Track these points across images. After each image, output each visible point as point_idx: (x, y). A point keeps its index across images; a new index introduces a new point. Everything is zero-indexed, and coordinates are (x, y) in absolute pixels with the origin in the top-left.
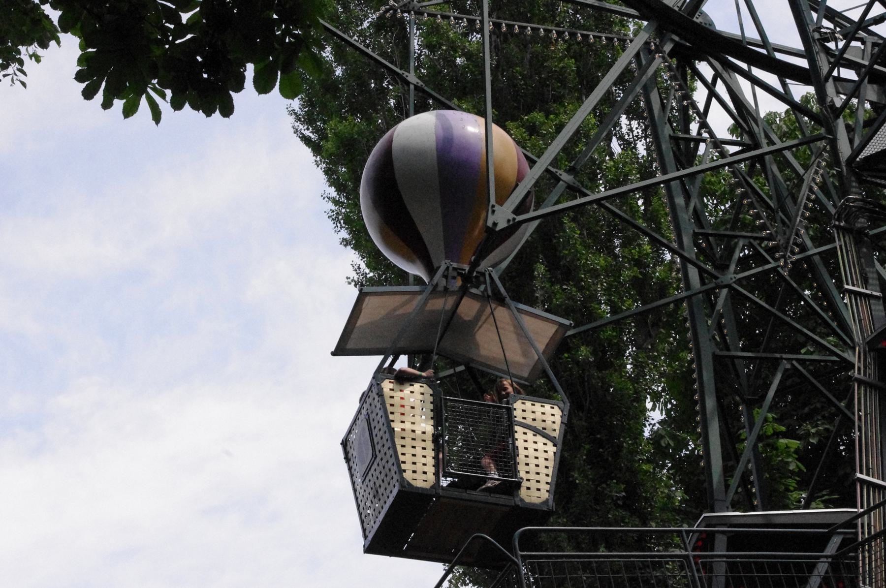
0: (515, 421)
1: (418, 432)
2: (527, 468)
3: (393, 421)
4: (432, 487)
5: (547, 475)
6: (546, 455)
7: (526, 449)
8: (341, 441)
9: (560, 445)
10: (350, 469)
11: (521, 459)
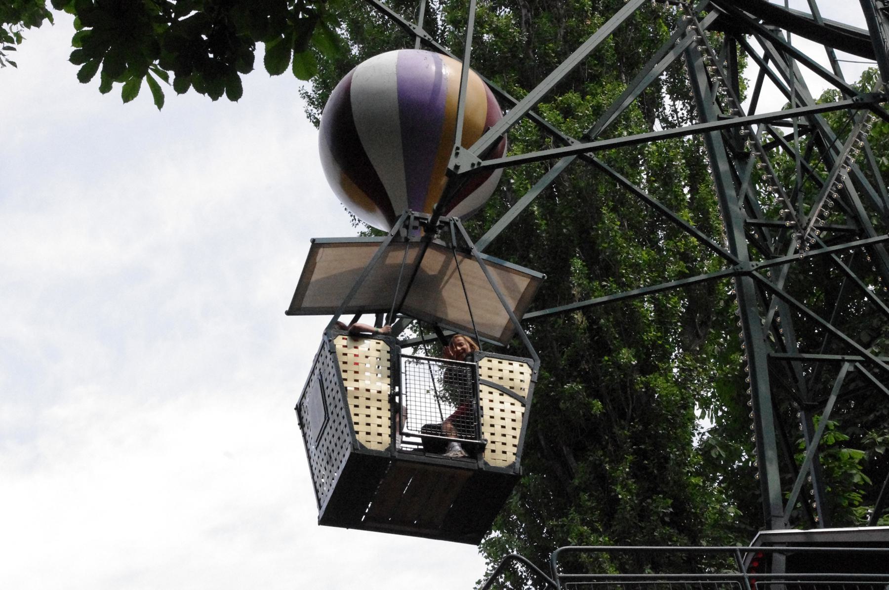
0: (479, 380)
1: (374, 391)
2: (492, 430)
3: (346, 380)
4: (387, 450)
5: (514, 437)
6: (513, 416)
7: (492, 409)
8: (295, 407)
9: (529, 406)
10: (304, 435)
11: (486, 419)
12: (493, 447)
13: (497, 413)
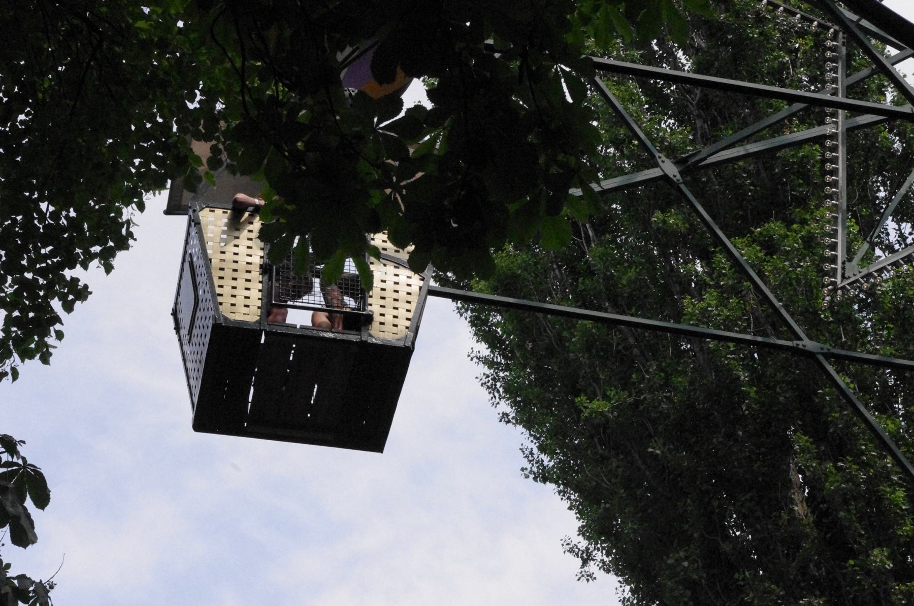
5: (408, 311)
6: (409, 289)
10: (180, 340)
12: (382, 319)
13: (389, 285)
